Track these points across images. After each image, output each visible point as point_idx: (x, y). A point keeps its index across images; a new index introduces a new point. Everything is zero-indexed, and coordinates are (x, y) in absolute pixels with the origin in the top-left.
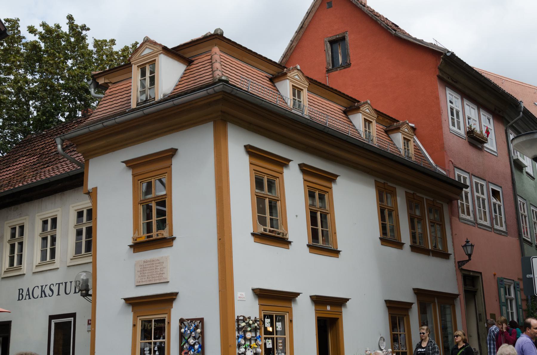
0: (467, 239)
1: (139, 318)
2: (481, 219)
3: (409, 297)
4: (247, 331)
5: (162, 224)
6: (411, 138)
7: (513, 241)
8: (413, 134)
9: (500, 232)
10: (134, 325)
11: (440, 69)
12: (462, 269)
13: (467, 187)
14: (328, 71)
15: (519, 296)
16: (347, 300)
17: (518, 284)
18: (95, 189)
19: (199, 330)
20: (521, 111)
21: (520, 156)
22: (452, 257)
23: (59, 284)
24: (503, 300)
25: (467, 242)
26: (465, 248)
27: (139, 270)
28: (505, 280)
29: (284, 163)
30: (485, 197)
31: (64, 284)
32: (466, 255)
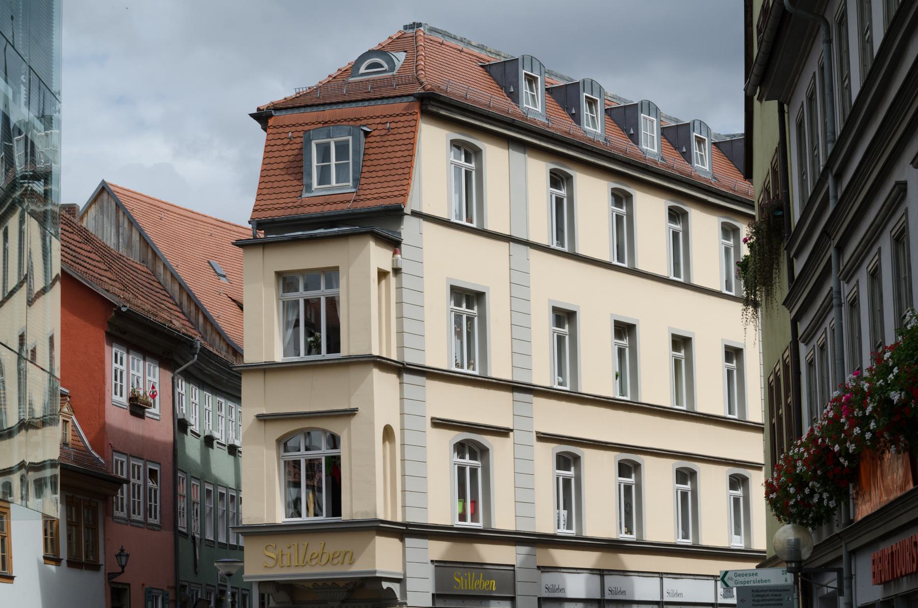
6: (70, 418)
7: (168, 535)
8: (72, 413)
9: (152, 527)
12: (113, 582)
17: (167, 595)
20: (196, 354)
22: (103, 568)
25: (122, 550)
26: (119, 558)
28: (154, 591)
30: (141, 482)
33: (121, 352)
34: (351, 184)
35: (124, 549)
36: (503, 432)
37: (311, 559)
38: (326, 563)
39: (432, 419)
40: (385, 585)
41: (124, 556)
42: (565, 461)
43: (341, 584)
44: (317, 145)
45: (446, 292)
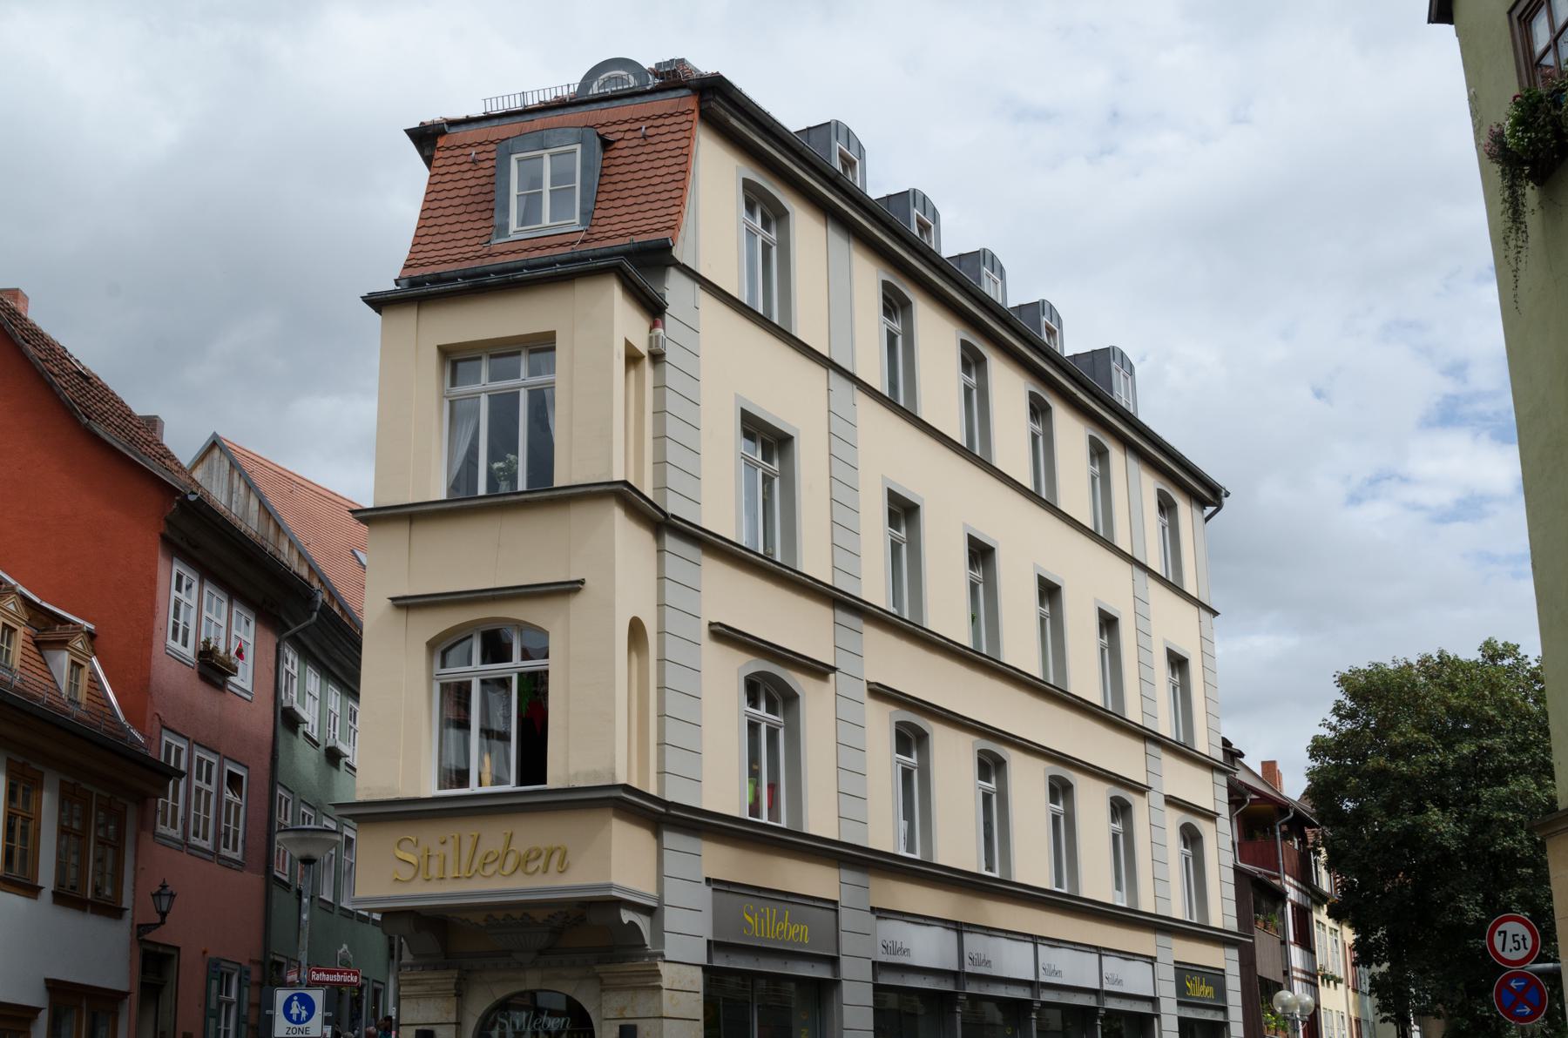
0: (164, 882)
2: (196, 835)
3: (33, 996)
6: (86, 661)
7: (255, 880)
8: (91, 654)
9: (228, 863)
11: (168, 522)
12: (144, 940)
13: (181, 774)
15: (246, 998)
17: (248, 973)
20: (315, 610)
21: (298, 702)
22: (128, 914)
24: (213, 1005)
25: (164, 887)
26: (157, 898)
28: (223, 964)
30: (212, 788)
32: (157, 912)
33: (189, 575)
34: (577, 220)
35: (167, 883)
36: (820, 671)
37: (484, 864)
38: (513, 873)
39: (711, 624)
40: (627, 916)
41: (165, 895)
42: (909, 740)
43: (540, 916)
44: (519, 161)
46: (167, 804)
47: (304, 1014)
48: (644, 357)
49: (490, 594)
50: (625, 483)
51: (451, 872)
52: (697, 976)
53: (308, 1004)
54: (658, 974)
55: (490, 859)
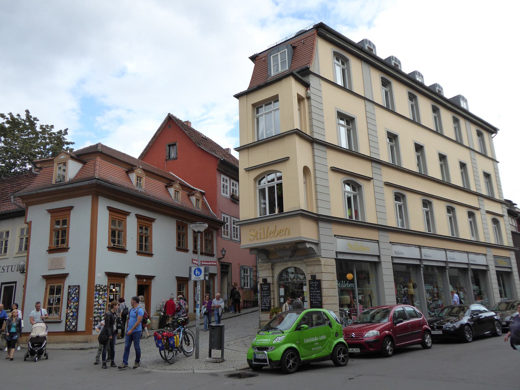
1: (49, 285)
2: (234, 237)
4: (100, 291)
5: (63, 242)
10: (46, 289)
11: (218, 166)
12: (220, 262)
14: (166, 160)
15: (252, 274)
16: (155, 276)
18: (31, 222)
19: (77, 291)
23: (8, 266)
24: (242, 276)
25: (223, 249)
27: (51, 262)
28: (244, 267)
29: (127, 214)
31: (11, 267)
33: (226, 178)
34: (287, 68)
36: (368, 179)
37: (270, 234)
40: (308, 246)
42: (398, 197)
45: (335, 115)
46: (225, 231)
47: (199, 273)
48: (304, 98)
49: (267, 164)
50: (297, 129)
51: (262, 237)
52: (334, 262)
53: (200, 270)
54: (320, 261)
55: (271, 233)
